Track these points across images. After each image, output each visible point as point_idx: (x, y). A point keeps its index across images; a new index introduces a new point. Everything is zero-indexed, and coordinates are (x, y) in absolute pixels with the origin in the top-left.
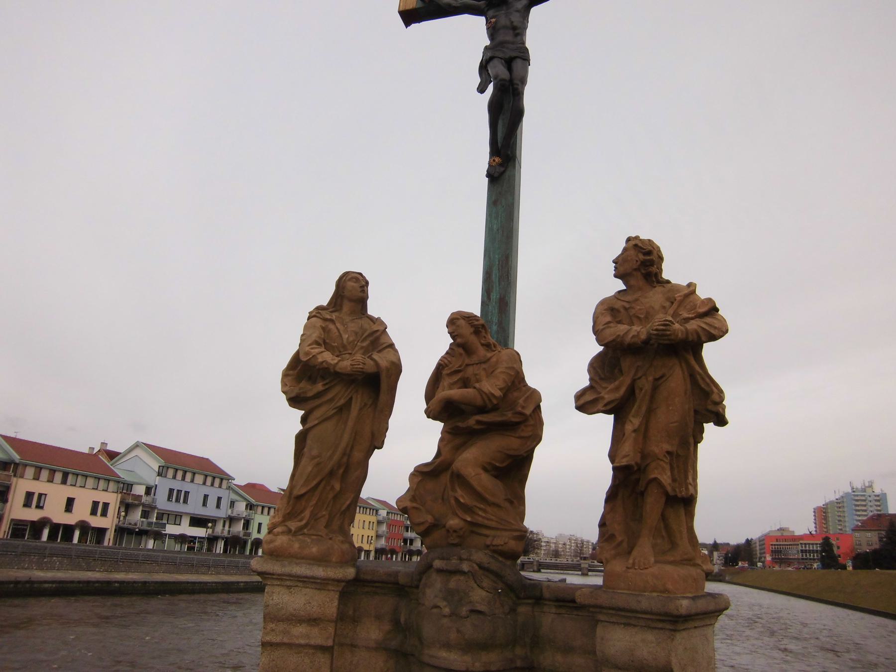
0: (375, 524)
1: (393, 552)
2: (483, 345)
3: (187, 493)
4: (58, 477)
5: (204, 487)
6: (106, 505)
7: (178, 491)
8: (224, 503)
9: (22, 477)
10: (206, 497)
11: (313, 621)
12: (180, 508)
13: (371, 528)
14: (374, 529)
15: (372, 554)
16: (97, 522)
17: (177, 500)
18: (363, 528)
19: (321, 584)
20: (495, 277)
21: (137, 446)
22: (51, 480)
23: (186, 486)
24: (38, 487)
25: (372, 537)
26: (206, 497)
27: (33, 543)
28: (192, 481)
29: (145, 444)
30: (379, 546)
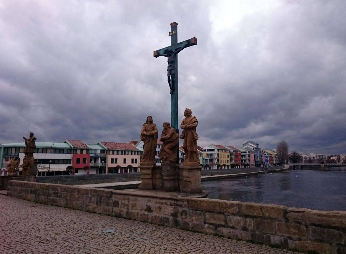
0: (229, 156)
1: (237, 165)
2: (169, 128)
4: (120, 152)
6: (136, 160)
11: (148, 174)
13: (228, 157)
14: (229, 157)
15: (230, 167)
16: (134, 165)
18: (225, 157)
19: (149, 169)
20: (173, 113)
22: (118, 154)
24: (115, 157)
25: (229, 160)
27: (116, 174)
30: (232, 163)
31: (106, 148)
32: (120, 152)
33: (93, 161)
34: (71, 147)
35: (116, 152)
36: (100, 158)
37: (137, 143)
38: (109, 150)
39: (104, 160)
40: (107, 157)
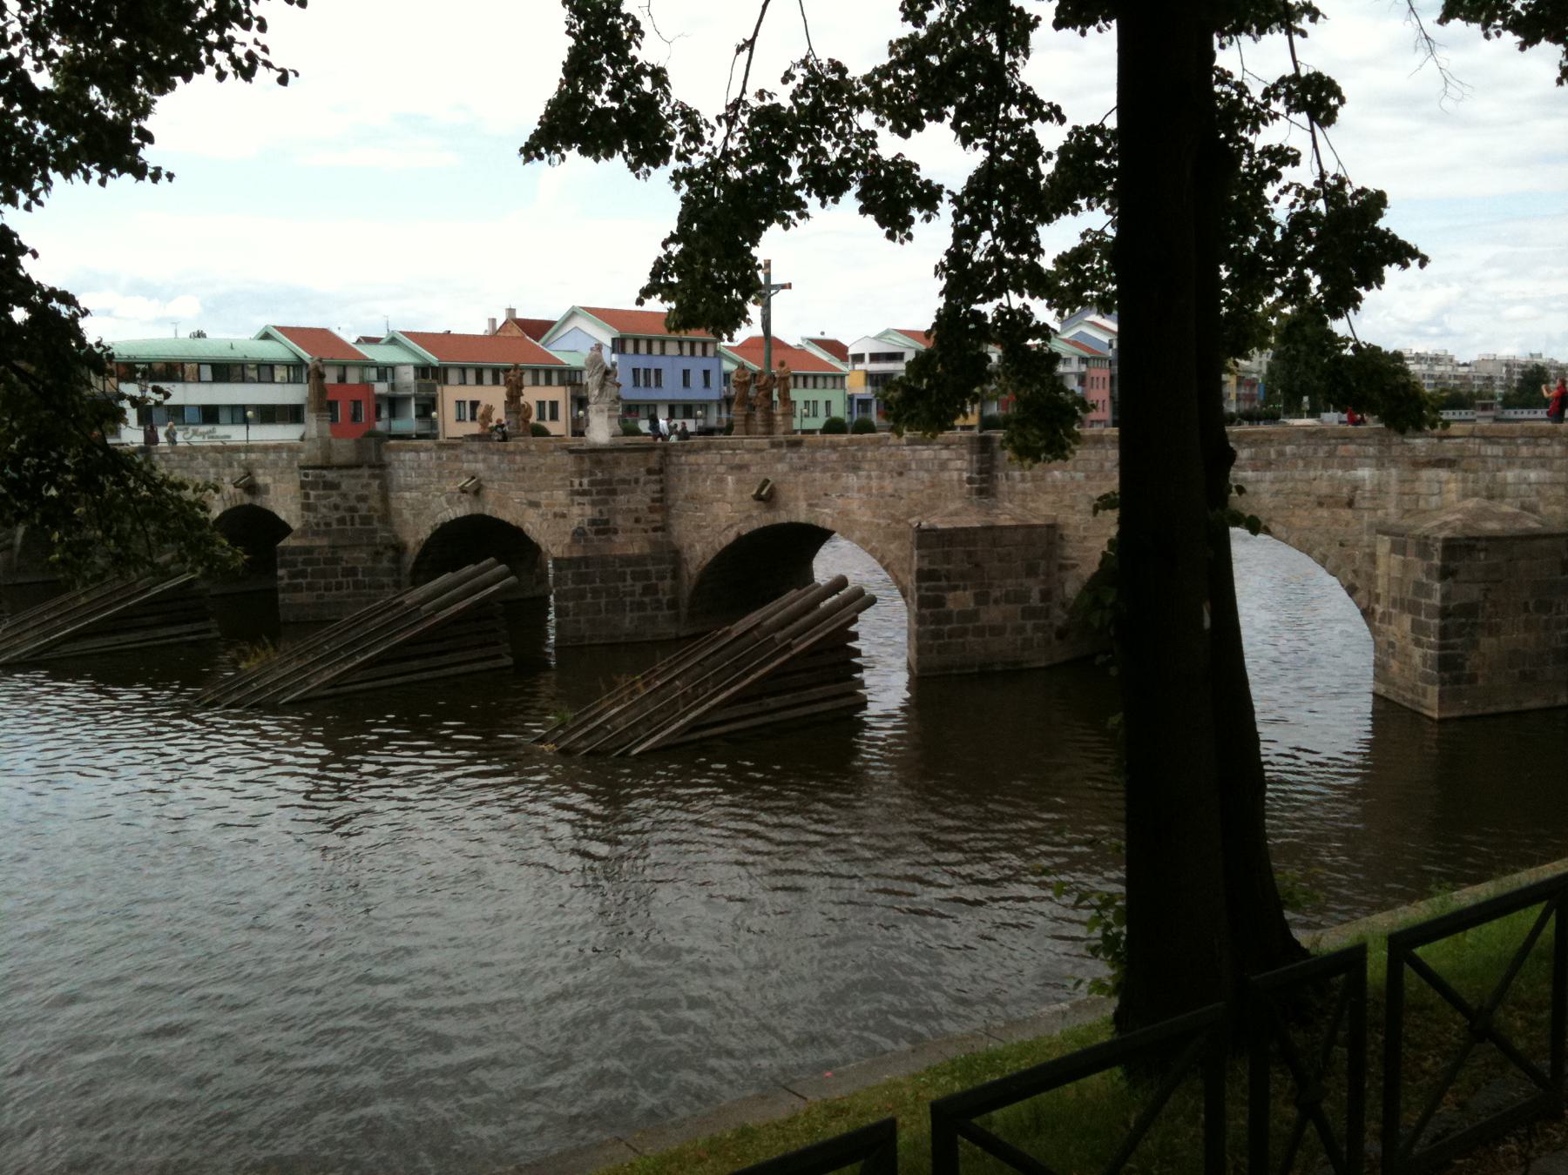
3: (658, 372)
4: (488, 376)
5: (680, 360)
6: (554, 405)
7: (647, 371)
8: (715, 379)
9: (446, 382)
10: (686, 373)
12: (652, 394)
17: (647, 384)
21: (572, 314)
22: (479, 381)
23: (656, 362)
26: (686, 373)
28: (663, 353)
29: (584, 308)
31: (433, 359)
32: (488, 376)
33: (384, 414)
34: (299, 358)
35: (471, 376)
36: (413, 403)
37: (550, 333)
38: (445, 369)
39: (427, 407)
40: (440, 398)
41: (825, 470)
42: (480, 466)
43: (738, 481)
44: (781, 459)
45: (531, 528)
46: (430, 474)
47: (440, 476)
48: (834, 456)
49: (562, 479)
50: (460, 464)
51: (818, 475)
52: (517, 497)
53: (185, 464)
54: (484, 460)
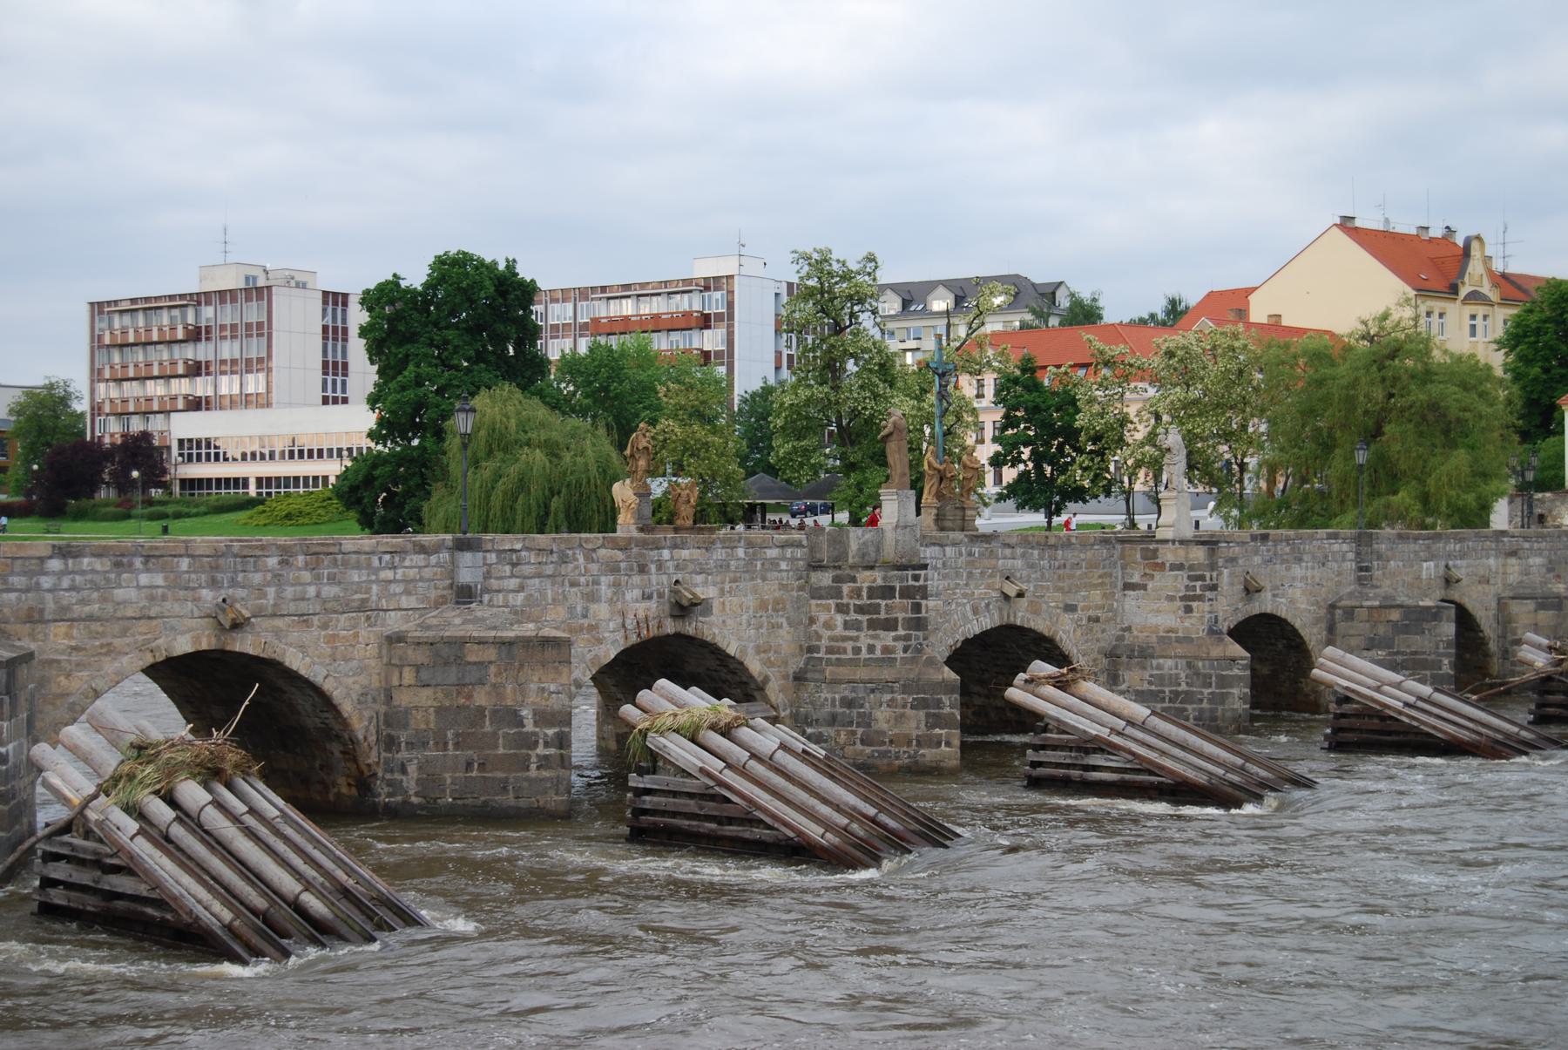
41: (1283, 561)
42: (1019, 563)
43: (1231, 575)
44: (1256, 553)
45: (1064, 637)
46: (958, 575)
47: (970, 575)
48: (1287, 549)
49: (1100, 577)
50: (993, 562)
51: (1278, 566)
52: (1053, 600)
53: (549, 570)
54: (1023, 556)
